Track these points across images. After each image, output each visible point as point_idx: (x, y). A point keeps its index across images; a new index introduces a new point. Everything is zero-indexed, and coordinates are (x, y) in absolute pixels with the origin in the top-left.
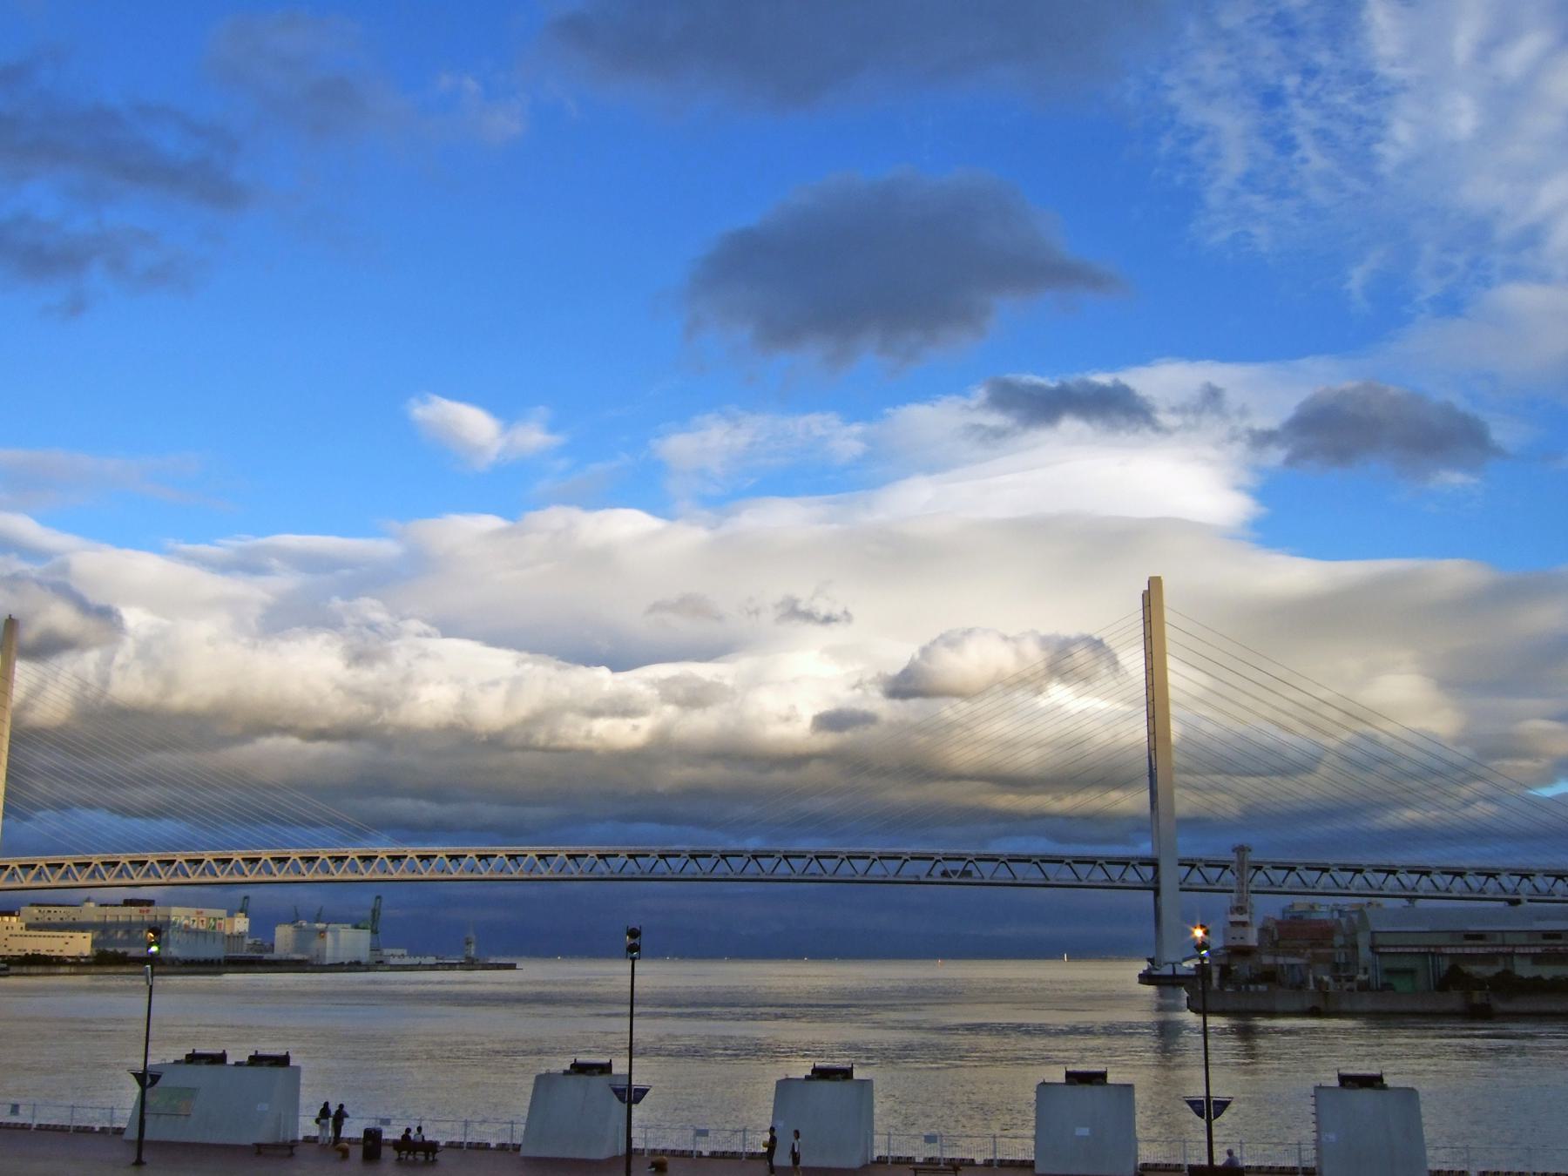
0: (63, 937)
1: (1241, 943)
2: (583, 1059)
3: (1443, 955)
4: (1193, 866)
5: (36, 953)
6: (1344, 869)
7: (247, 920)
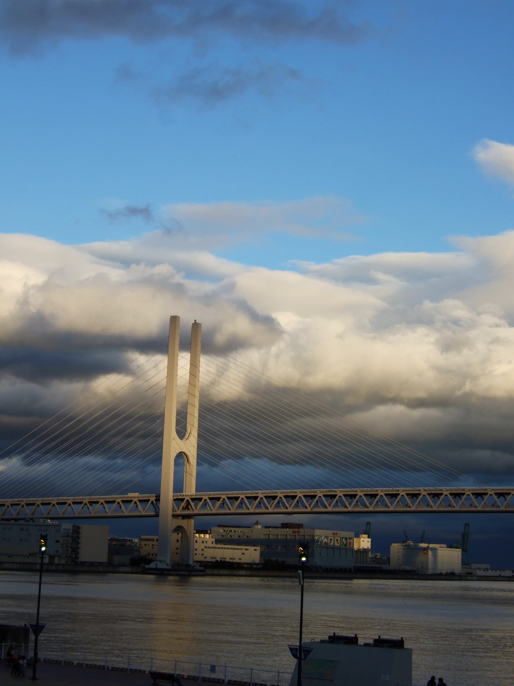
0: (240, 549)
2: (340, 633)
5: (223, 560)
7: (370, 540)
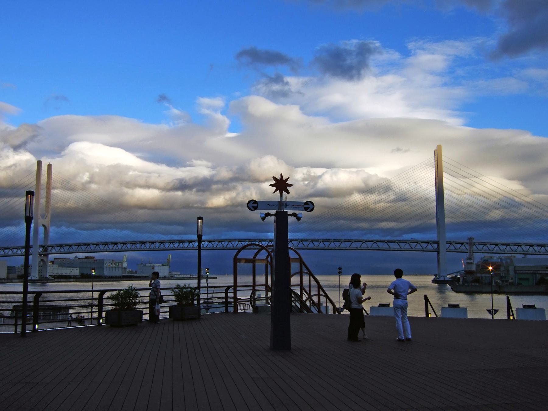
0: (70, 269)
1: (471, 270)
3: (538, 273)
4: (451, 244)
6: (503, 244)
